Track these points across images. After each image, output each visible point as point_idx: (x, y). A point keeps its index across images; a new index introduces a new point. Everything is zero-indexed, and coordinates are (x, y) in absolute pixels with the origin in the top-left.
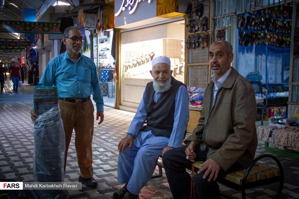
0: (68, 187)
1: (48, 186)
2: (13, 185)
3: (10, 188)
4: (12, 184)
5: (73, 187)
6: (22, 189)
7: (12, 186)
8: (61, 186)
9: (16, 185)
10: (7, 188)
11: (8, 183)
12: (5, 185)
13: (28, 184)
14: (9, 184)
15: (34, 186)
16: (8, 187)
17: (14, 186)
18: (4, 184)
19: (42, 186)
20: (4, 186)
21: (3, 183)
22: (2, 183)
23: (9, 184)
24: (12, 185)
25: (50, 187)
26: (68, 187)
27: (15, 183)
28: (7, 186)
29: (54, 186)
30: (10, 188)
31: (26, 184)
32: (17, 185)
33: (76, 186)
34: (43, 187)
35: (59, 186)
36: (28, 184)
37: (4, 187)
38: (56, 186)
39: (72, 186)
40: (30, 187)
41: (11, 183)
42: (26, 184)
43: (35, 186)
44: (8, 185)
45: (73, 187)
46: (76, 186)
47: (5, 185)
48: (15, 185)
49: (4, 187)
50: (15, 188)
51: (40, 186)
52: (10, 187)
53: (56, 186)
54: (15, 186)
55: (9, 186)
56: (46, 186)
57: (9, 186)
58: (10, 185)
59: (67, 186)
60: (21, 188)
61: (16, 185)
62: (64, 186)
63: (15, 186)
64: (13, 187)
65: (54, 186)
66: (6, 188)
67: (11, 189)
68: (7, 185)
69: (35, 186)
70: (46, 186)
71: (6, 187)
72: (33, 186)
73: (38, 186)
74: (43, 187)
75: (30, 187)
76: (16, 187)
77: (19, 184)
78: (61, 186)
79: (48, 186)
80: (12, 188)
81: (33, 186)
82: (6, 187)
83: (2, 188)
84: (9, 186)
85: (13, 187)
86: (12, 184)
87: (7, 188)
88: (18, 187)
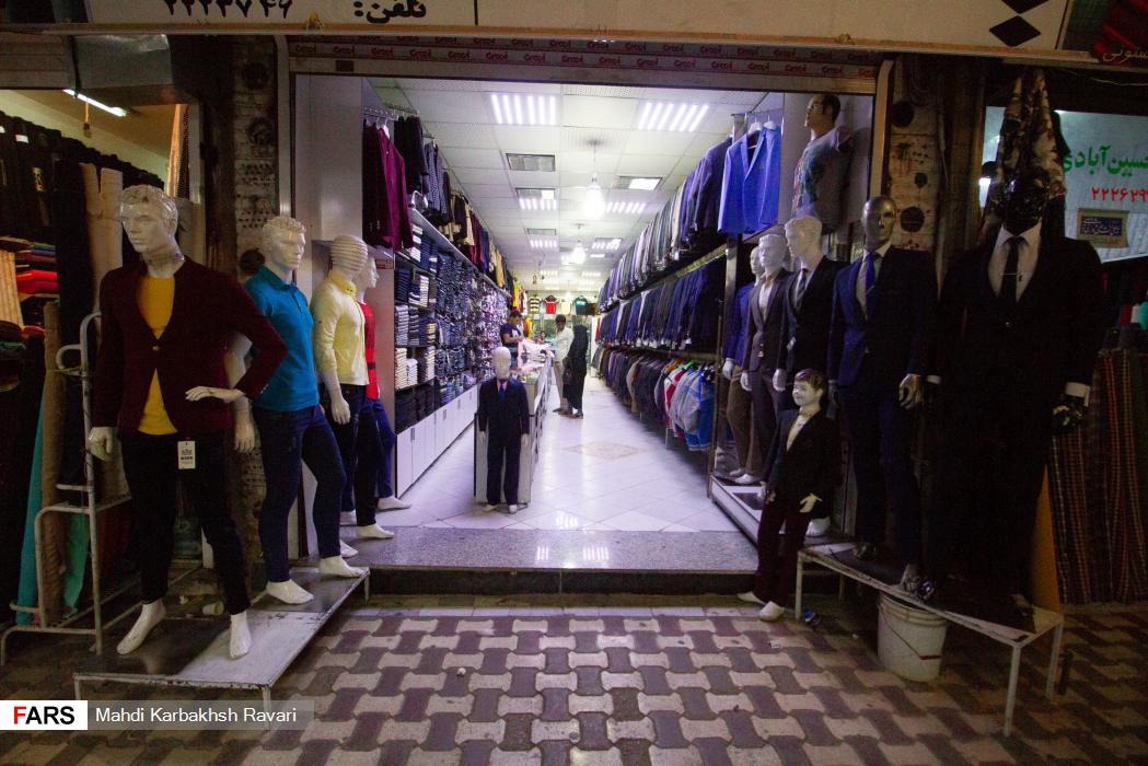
1: (184, 717)
2: (51, 712)
3: (40, 722)
4: (46, 709)
5: (281, 718)
7: (46, 715)
8: (233, 716)
9: (60, 713)
10: (28, 722)
11: (29, 704)
12: (20, 711)
13: (108, 709)
14: (34, 709)
15: (130, 717)
16: (30, 718)
17: (53, 716)
18: (16, 709)
19: (161, 716)
20: (16, 715)
22: (7, 706)
23: (34, 709)
24: (46, 712)
25: (193, 718)
26: (261, 718)
27: (60, 704)
28: (27, 716)
29: (207, 716)
30: (40, 722)
32: (67, 711)
33: (291, 716)
34: (167, 718)
35: (227, 716)
36: (108, 709)
37: (16, 722)
38: (213, 716)
39: (276, 716)
40: (115, 718)
41: (40, 705)
42: (98, 710)
43: (135, 717)
44: (31, 713)
45: (281, 718)
47: (20, 711)
48: (56, 713)
49: (16, 722)
50: (57, 722)
51: (153, 715)
52: (38, 718)
53: (213, 716)
54: (59, 716)
55: (33, 715)
56: (177, 716)
57: (34, 715)
58: (37, 714)
59: (256, 716)
60: (81, 723)
61: (60, 713)
62: (246, 715)
63: (59, 716)
64: (49, 719)
65: (207, 716)
66: (22, 726)
67: (43, 727)
68: (27, 712)
69: (135, 717)
70: (177, 716)
71: (22, 720)
72: (126, 716)
73: (147, 715)
74: (167, 718)
75: (115, 718)
76: (62, 720)
77: (72, 710)
78: (233, 716)
79: (184, 717)
80: (46, 722)
81: (126, 716)
82: (22, 720)
83: (9, 725)
84: (34, 715)
85: (49, 719)
86: (46, 709)
87: (28, 722)
88: (68, 719)
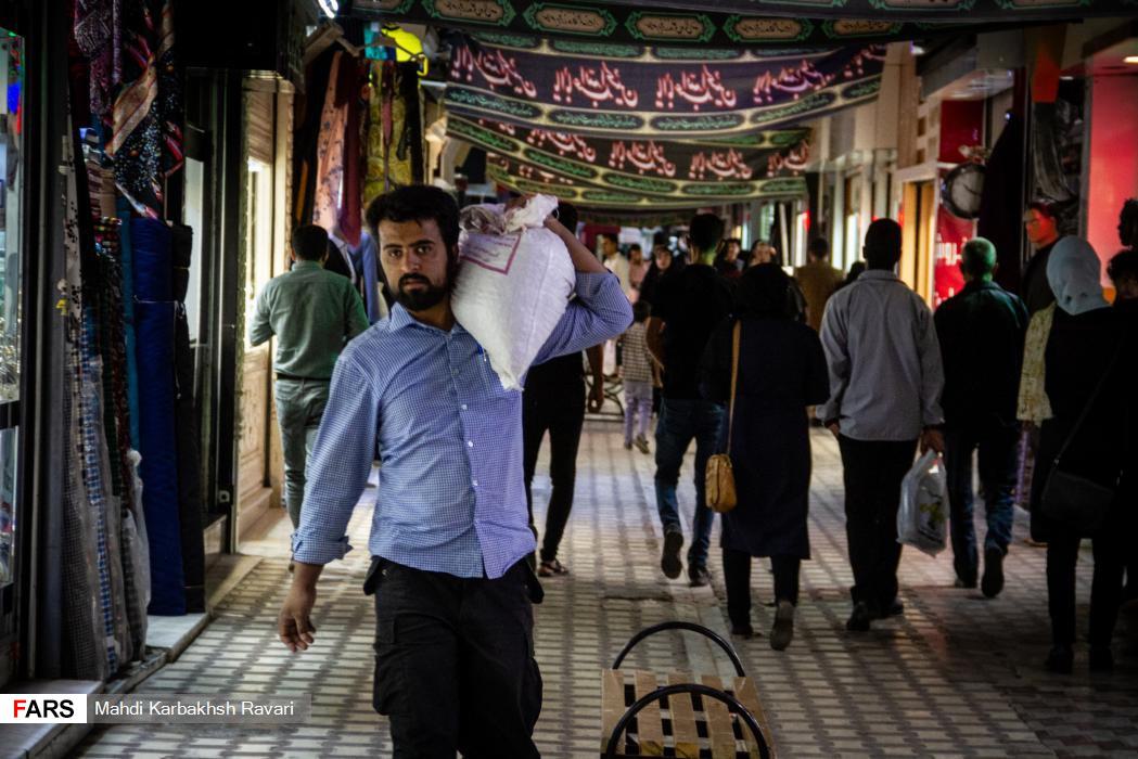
0: (259, 712)
1: (182, 710)
2: (51, 705)
3: (40, 716)
4: (46, 702)
5: (278, 712)
6: (84, 720)
7: (46, 709)
9: (59, 706)
10: (27, 715)
11: (29, 697)
12: (19, 705)
13: (107, 703)
14: (33, 703)
15: (129, 711)
16: (30, 712)
17: (52, 710)
18: (16, 702)
19: (160, 711)
20: (16, 709)
21: (9, 699)
22: (8, 699)
23: (33, 703)
24: (45, 705)
25: (192, 712)
26: (259, 712)
27: (59, 698)
28: (27, 710)
29: (205, 710)
30: (40, 716)
31: (97, 703)
32: (66, 704)
33: (289, 710)
34: (165, 712)
36: (107, 703)
37: (16, 715)
38: (211, 709)
39: (273, 709)
40: (114, 712)
41: (40, 698)
42: (97, 703)
43: (134, 710)
44: (31, 707)
45: (278, 712)
46: (289, 710)
47: (19, 705)
48: (56, 707)
49: (16, 715)
50: (56, 716)
52: (37, 712)
53: (211, 709)
54: (59, 710)
55: (33, 709)
56: (176, 709)
57: (33, 709)
58: (36, 707)
59: (254, 709)
60: (80, 717)
61: (59, 706)
62: (244, 709)
63: (59, 710)
64: (49, 712)
65: (205, 710)
66: (22, 719)
67: (42, 720)
68: (27, 705)
69: (134, 710)
70: (176, 709)
72: (125, 709)
73: (146, 710)
74: (165, 712)
75: (114, 712)
76: (62, 714)
77: (71, 703)
79: (182, 710)
80: (45, 715)
81: (125, 709)
83: (8, 718)
84: (33, 709)
85: (49, 712)
86: (46, 702)
87: (27, 715)
88: (67, 712)
